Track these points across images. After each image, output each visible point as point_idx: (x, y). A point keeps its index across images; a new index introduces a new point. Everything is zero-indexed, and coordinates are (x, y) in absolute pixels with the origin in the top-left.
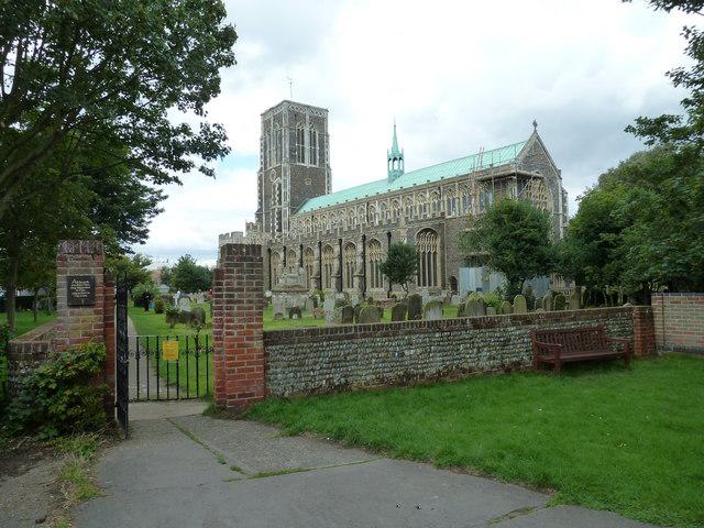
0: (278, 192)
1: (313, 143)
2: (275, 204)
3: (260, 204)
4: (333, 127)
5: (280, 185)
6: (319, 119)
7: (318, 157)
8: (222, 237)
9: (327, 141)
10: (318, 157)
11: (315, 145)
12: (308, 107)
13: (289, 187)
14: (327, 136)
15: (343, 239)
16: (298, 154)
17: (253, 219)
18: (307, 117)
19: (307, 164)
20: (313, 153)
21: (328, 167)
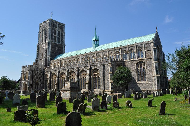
0: (45, 52)
1: (59, 35)
2: (44, 55)
3: (38, 56)
4: (66, 31)
5: (46, 49)
6: (62, 27)
7: (61, 40)
8: (24, 67)
9: (64, 35)
10: (61, 40)
11: (60, 36)
12: (58, 22)
13: (50, 50)
14: (64, 33)
15: (80, 68)
16: (53, 38)
17: (34, 62)
18: (58, 26)
19: (57, 42)
20: (59, 39)
21: (64, 44)
